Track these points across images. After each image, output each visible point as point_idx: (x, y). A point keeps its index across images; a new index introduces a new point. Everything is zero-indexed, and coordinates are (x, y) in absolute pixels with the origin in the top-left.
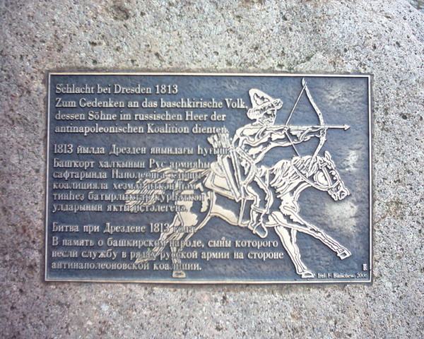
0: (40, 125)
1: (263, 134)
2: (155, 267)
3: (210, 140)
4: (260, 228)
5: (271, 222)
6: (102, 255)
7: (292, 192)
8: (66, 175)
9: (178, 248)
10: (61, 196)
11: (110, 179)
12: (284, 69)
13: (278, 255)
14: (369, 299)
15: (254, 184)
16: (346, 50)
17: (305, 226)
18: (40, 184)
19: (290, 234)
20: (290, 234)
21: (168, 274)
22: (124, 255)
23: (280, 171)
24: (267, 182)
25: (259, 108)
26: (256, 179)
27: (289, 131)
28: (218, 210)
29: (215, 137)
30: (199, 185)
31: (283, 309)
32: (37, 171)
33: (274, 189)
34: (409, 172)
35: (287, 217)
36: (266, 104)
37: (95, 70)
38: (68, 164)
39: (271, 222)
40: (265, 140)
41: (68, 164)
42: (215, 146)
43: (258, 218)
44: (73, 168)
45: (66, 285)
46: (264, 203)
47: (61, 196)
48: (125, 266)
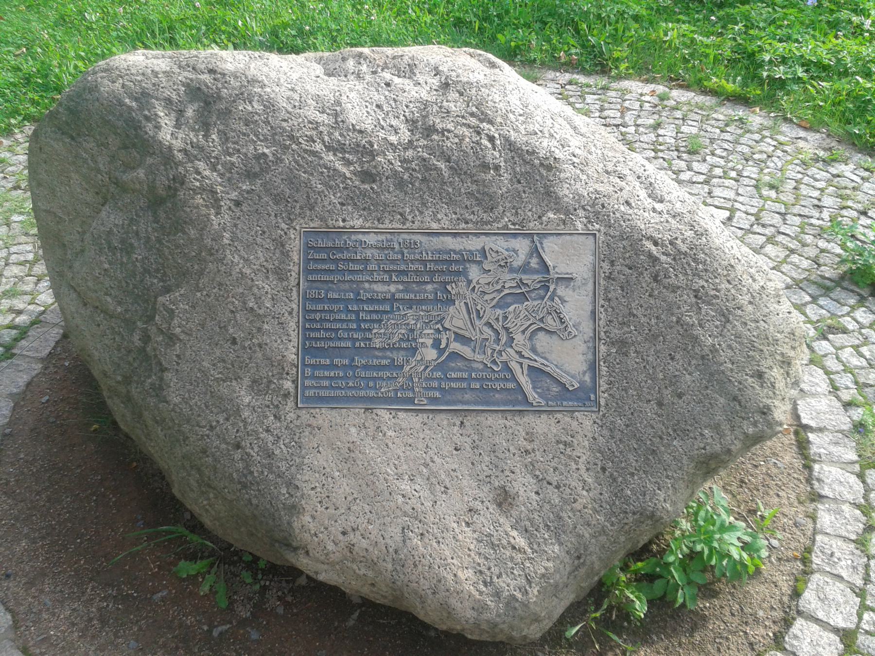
0: (293, 274)
1: (497, 282)
2: (399, 395)
3: (449, 288)
4: (494, 362)
5: (504, 357)
6: (351, 384)
7: (523, 332)
8: (318, 316)
9: (419, 378)
10: (312, 335)
11: (358, 321)
12: (517, 227)
13: (511, 385)
14: (596, 425)
15: (488, 324)
16: (575, 210)
17: (536, 361)
18: (293, 325)
19: (522, 368)
20: (522, 368)
21: (411, 401)
22: (371, 384)
23: (512, 315)
24: (500, 323)
25: (494, 260)
26: (490, 321)
27: (521, 279)
28: (456, 346)
29: (453, 285)
30: (439, 326)
31: (516, 433)
32: (290, 313)
33: (507, 329)
34: (634, 315)
35: (519, 353)
36: (500, 257)
37: (344, 227)
38: (320, 307)
39: (504, 357)
40: (499, 287)
41: (320, 307)
42: (453, 292)
43: (492, 353)
45: (318, 410)
46: (498, 340)
47: (312, 335)
48: (372, 393)
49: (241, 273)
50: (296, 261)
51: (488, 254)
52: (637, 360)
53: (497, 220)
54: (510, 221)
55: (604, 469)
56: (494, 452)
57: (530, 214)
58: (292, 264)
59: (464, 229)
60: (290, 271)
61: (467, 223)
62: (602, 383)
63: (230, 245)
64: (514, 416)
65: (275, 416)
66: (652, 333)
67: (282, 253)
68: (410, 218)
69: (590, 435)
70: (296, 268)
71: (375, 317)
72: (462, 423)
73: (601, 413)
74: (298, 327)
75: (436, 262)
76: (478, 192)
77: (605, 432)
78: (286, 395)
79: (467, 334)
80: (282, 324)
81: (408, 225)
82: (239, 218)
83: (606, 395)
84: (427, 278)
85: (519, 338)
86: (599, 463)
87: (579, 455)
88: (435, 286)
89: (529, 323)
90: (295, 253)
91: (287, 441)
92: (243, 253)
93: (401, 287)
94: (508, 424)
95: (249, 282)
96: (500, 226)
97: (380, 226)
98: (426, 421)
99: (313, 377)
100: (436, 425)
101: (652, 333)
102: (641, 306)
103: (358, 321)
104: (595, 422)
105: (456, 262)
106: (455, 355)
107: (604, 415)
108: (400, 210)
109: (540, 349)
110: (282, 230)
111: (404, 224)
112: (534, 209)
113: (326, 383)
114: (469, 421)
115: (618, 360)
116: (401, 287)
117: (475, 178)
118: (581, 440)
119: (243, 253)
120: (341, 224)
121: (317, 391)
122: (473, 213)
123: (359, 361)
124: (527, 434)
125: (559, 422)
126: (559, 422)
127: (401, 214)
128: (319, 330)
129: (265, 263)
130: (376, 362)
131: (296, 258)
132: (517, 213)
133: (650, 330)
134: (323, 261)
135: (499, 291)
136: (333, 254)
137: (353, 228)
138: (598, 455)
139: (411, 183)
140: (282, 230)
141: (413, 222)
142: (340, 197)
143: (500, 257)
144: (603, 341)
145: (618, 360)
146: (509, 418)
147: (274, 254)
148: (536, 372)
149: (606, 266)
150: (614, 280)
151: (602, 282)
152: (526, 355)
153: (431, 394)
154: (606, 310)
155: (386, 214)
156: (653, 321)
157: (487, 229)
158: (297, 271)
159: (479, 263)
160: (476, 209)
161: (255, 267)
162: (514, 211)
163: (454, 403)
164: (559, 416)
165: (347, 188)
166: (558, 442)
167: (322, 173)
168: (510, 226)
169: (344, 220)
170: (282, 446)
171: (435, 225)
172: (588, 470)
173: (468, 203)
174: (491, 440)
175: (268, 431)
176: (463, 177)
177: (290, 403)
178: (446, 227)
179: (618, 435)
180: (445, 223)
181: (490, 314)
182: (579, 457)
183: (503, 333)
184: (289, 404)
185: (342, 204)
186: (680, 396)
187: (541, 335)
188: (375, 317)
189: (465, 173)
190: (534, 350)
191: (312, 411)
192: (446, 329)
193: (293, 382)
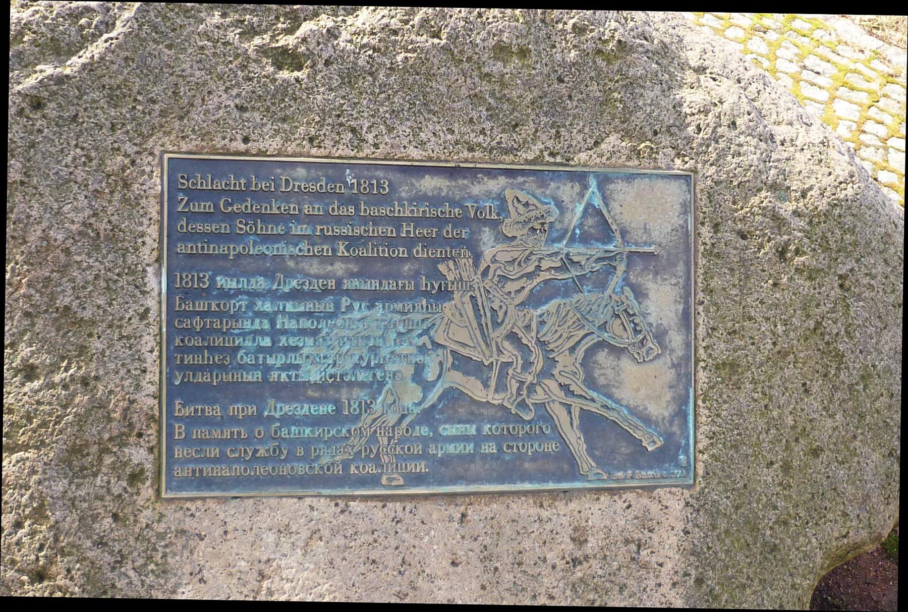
0: (147, 239)
1: (527, 259)
2: (353, 470)
3: (442, 268)
4: (523, 405)
5: (540, 396)
6: (262, 452)
7: (572, 349)
8: (197, 323)
9: (389, 439)
10: (188, 359)
11: (274, 333)
12: (559, 159)
13: (552, 447)
14: (690, 510)
15: (512, 337)
16: (656, 133)
17: (593, 400)
18: (148, 341)
19: (570, 413)
20: (570, 413)
21: (374, 481)
22: (300, 452)
23: (554, 318)
24: (533, 334)
25: (522, 219)
26: (515, 330)
27: (567, 255)
28: (455, 379)
29: (451, 263)
30: (425, 339)
31: (559, 529)
32: (144, 316)
33: (542, 344)
34: (750, 318)
35: (565, 388)
36: (533, 214)
37: (246, 153)
38: (201, 306)
39: (540, 396)
40: (531, 269)
41: (201, 306)
42: (450, 277)
43: (519, 389)
44: (202, 315)
45: (199, 503)
46: (527, 365)
47: (188, 359)
48: (301, 469)
49: (45, 238)
50: (155, 216)
51: (511, 208)
52: (756, 396)
53: (525, 145)
54: (547, 148)
55: (699, 581)
56: (520, 564)
57: (580, 138)
58: (146, 221)
59: (466, 161)
60: (143, 235)
61: (471, 149)
62: (700, 437)
63: (22, 183)
64: (555, 500)
65: (115, 517)
66: (778, 348)
67: (125, 200)
68: (370, 137)
69: (680, 526)
70: (153, 231)
71: (306, 324)
72: (464, 515)
73: (698, 489)
74: (160, 344)
75: (418, 222)
76: (492, 94)
77: (702, 519)
78: (136, 477)
79: (476, 356)
80: (128, 338)
81: (367, 151)
82: (40, 131)
83: (706, 456)
84: (402, 252)
85: (565, 362)
86: (693, 572)
87: (661, 561)
88: (416, 266)
89: (582, 333)
90: (153, 201)
91: (140, 562)
92: (49, 200)
93: (354, 267)
94: (545, 514)
95: (62, 257)
96: (530, 156)
97: (314, 151)
98: (400, 514)
99: (187, 441)
100: (418, 523)
101: (778, 348)
102: (762, 303)
103: (274, 333)
104: (687, 504)
105: (457, 222)
106: (453, 396)
107: (702, 492)
108: (353, 123)
109: (602, 381)
110: (126, 155)
111: (359, 148)
112: (587, 130)
113: (214, 452)
114: (477, 513)
115: (725, 396)
116: (354, 267)
117: (486, 70)
118: (665, 536)
119: (49, 200)
120: (242, 147)
121: (198, 467)
122: (483, 132)
123: (278, 409)
124: (576, 529)
125: (629, 506)
126: (629, 506)
127: (353, 130)
128: (199, 349)
129: (93, 220)
130: (305, 409)
131: (154, 213)
132: (558, 135)
133: (774, 344)
134: (206, 216)
135: (530, 276)
136: (227, 204)
137: (261, 153)
138: (692, 558)
139: (371, 74)
140: (126, 155)
141: (376, 146)
142: (238, 95)
143: (533, 214)
144: (702, 364)
145: (725, 396)
146: (545, 504)
147: (110, 202)
148: (591, 423)
149: (706, 232)
150: (718, 256)
151: (702, 261)
152: (578, 392)
153: (411, 467)
154: (707, 310)
155: (326, 130)
156: (780, 328)
157: (507, 162)
158: (155, 235)
159: (495, 224)
160: (488, 125)
161: (74, 228)
162: (554, 131)
163: (454, 480)
164: (630, 496)
165: (250, 79)
166: (627, 542)
167: (202, 48)
168: (547, 158)
169: (246, 140)
170: (131, 573)
171: (415, 153)
172: (674, 585)
173: (474, 115)
174: (514, 544)
175: (101, 543)
176: (466, 66)
177: (147, 490)
178: (434, 155)
179: (723, 525)
180: (434, 149)
181: (514, 320)
182: (661, 565)
183: (536, 351)
184: (143, 492)
185: (241, 109)
186: (816, 452)
187: (602, 356)
188: (306, 324)
189: (469, 59)
190: (590, 382)
191: (188, 505)
192: (436, 345)
193: (151, 450)
